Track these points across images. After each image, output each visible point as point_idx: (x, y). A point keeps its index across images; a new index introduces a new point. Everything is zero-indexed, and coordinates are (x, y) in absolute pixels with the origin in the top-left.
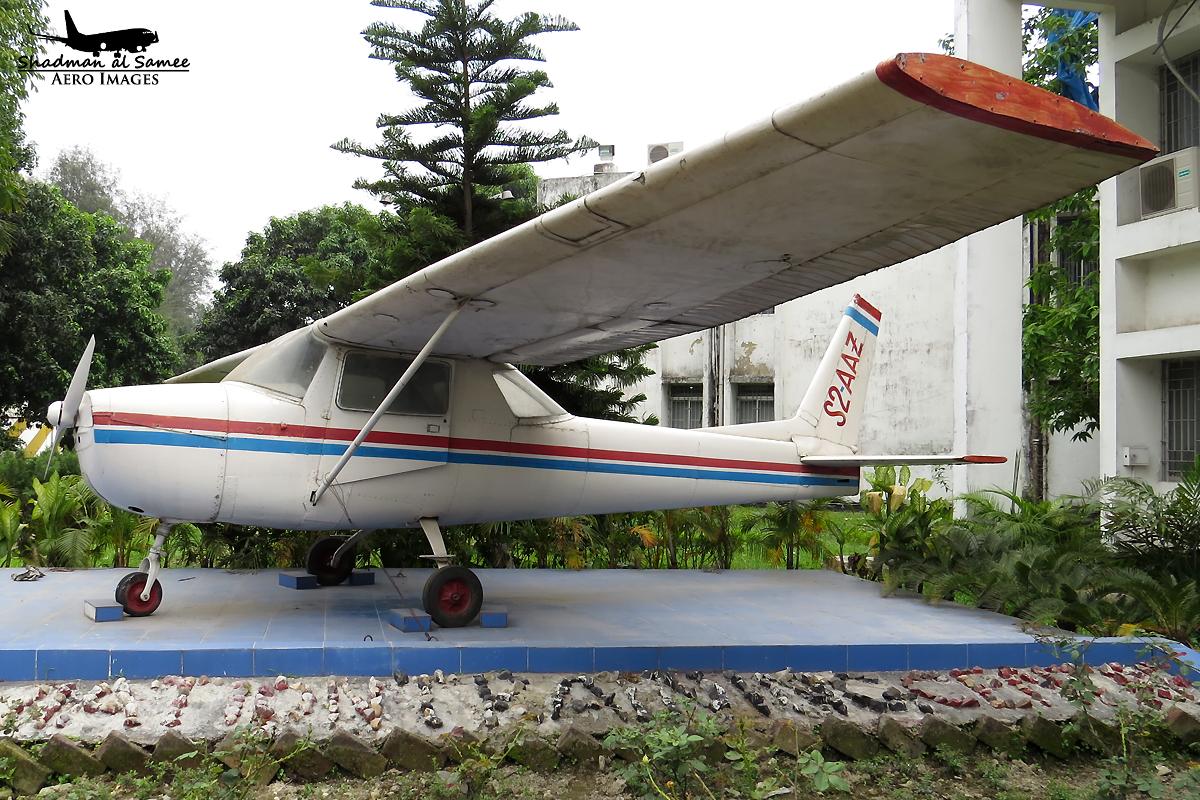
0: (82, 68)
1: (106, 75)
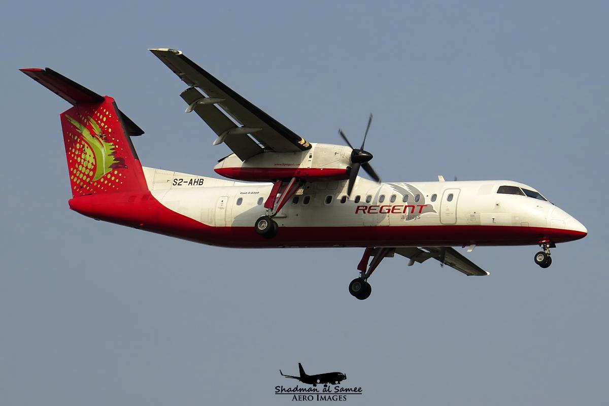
0: (307, 392)
1: (320, 396)
